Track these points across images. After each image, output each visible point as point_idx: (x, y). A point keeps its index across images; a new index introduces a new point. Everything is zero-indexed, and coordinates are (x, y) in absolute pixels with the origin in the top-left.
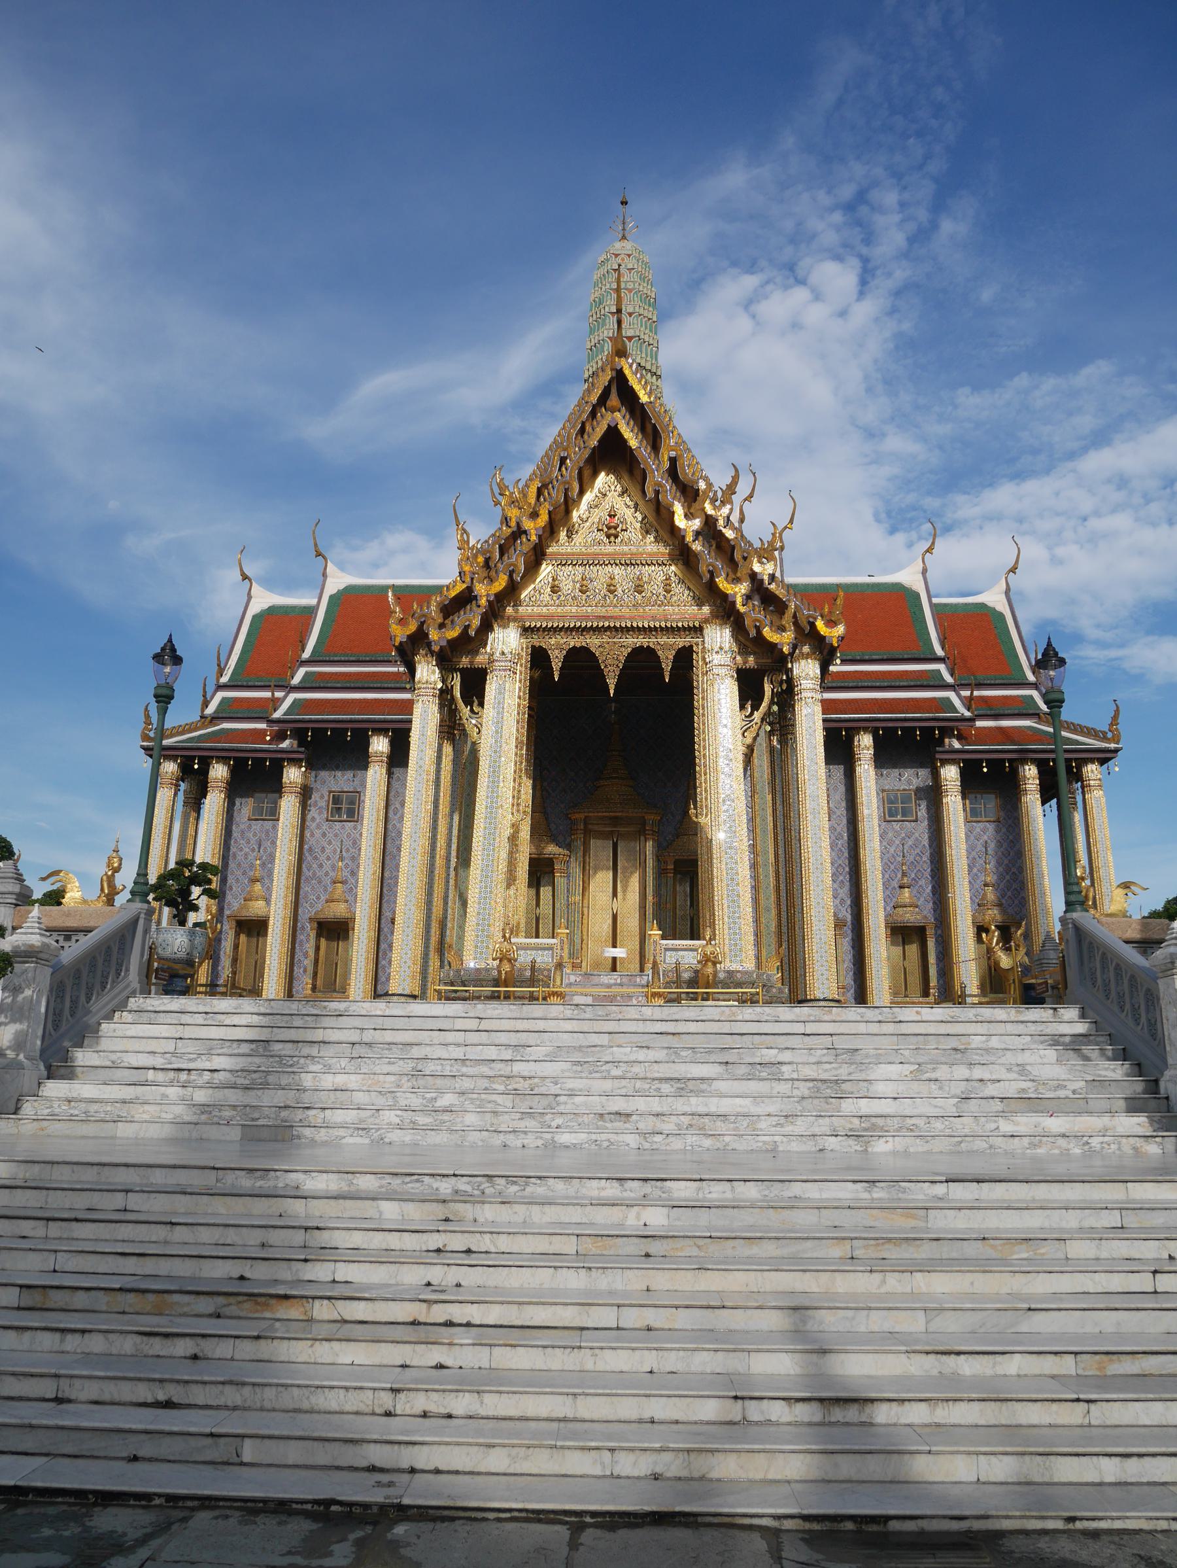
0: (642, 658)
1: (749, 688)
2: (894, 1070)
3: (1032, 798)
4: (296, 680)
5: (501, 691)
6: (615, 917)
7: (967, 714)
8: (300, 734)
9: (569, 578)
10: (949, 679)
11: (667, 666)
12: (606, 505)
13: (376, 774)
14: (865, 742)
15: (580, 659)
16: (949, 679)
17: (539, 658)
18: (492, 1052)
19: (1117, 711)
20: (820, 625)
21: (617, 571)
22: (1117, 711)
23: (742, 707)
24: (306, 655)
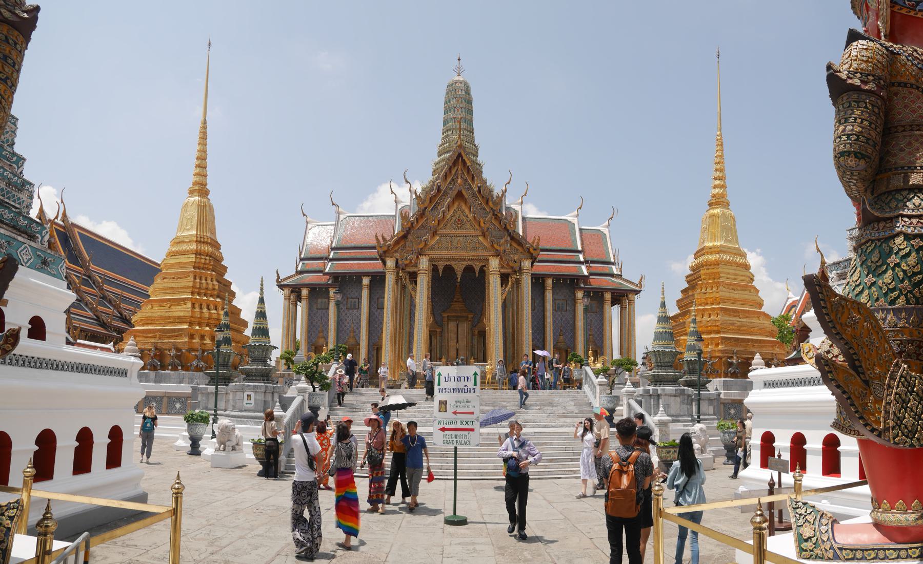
0: (469, 269)
1: (504, 278)
11: (477, 273)
14: (549, 282)
15: (449, 269)
17: (435, 269)
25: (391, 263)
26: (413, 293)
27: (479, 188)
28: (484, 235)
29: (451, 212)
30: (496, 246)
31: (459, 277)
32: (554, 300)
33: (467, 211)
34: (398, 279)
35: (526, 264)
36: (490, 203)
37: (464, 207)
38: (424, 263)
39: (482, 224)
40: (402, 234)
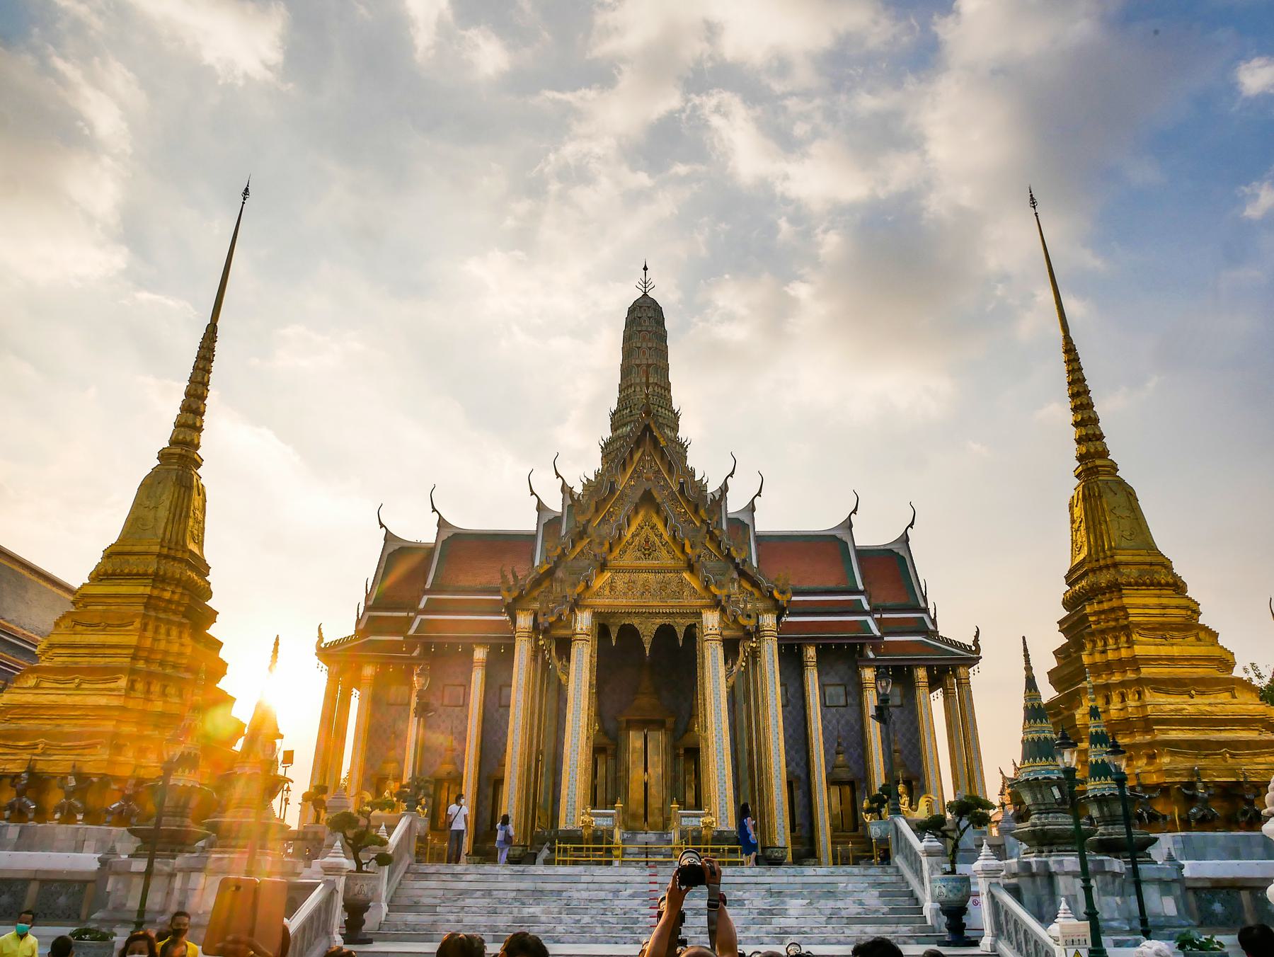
0: (665, 632)
1: (731, 648)
2: (800, 902)
3: (922, 692)
4: (422, 606)
5: (581, 654)
6: (646, 785)
7: (878, 634)
8: (427, 646)
9: (621, 581)
10: (867, 607)
11: (681, 637)
12: (643, 534)
13: (478, 676)
14: (811, 652)
16: (867, 607)
17: (602, 631)
18: (602, 895)
19: (978, 632)
20: (775, 593)
21: (651, 576)
22: (978, 632)
23: (726, 663)
24: (427, 586)
25: (524, 621)
26: (564, 678)
27: (682, 485)
28: (691, 568)
29: (633, 528)
30: (713, 588)
31: (647, 647)
32: (822, 687)
33: (660, 526)
34: (537, 651)
35: (769, 621)
36: (702, 512)
37: (655, 520)
38: (584, 621)
39: (688, 549)
40: (546, 567)
